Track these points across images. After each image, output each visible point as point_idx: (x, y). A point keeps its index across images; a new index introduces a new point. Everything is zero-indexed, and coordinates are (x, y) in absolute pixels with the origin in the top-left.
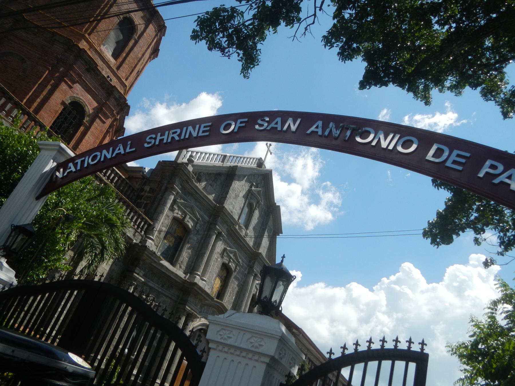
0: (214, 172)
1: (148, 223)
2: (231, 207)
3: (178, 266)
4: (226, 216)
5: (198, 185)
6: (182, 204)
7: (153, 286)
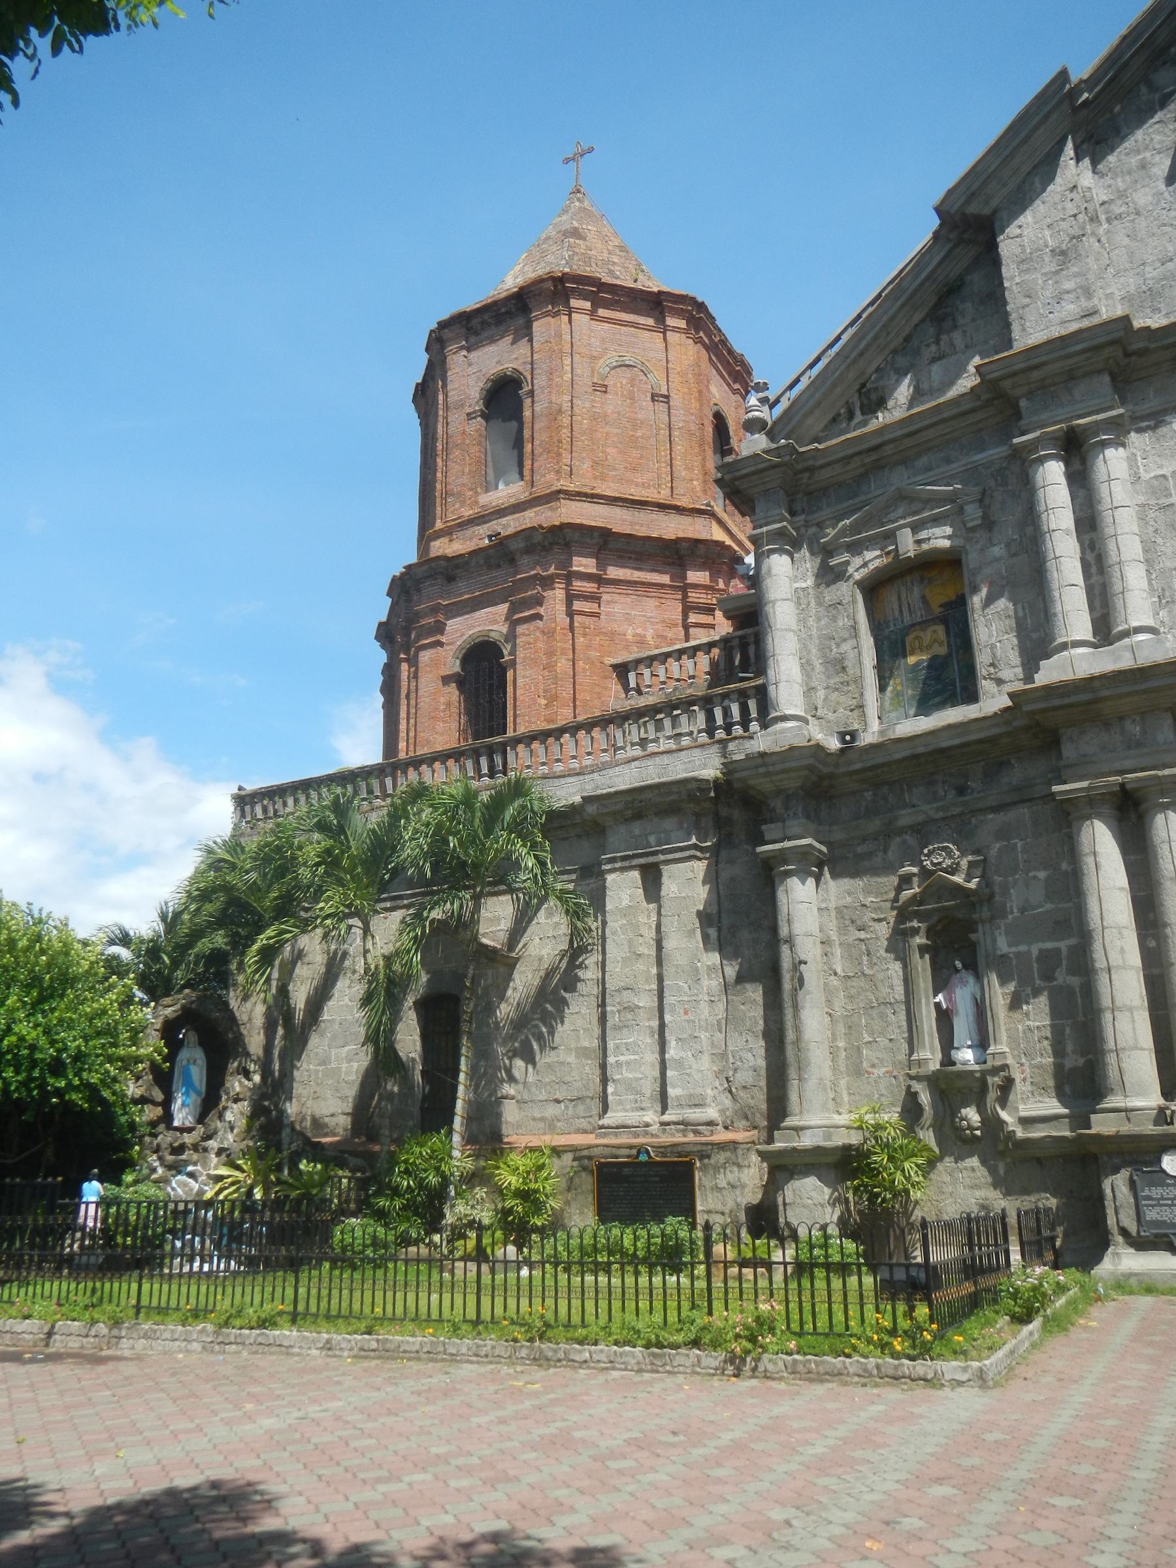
0: (918, 317)
1: (753, 692)
2: (1070, 308)
3: (986, 685)
4: (1036, 367)
5: (882, 418)
6: (855, 529)
7: (920, 818)
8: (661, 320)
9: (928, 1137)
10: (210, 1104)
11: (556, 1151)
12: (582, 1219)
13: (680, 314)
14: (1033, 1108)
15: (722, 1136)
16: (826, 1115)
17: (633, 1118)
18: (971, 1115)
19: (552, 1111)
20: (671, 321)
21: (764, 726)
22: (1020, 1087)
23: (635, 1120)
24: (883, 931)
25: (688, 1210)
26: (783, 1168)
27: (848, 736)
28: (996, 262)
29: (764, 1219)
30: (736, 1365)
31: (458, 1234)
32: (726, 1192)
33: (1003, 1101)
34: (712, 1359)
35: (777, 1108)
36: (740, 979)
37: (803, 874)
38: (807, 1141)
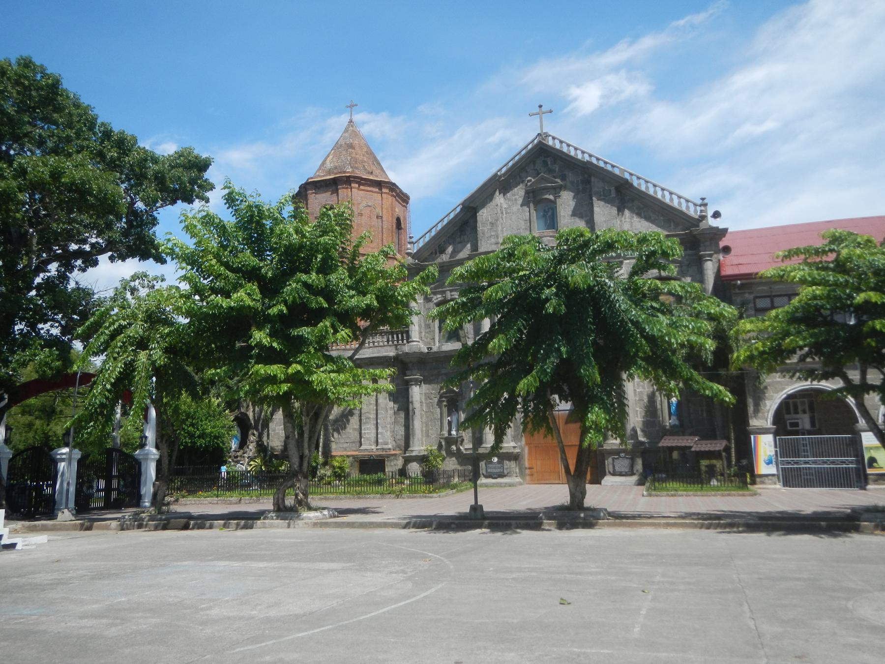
8: (381, 189)
9: (444, 453)
10: (243, 444)
11: (348, 456)
12: (355, 474)
13: (387, 187)
14: (467, 446)
15: (393, 452)
16: (419, 447)
17: (368, 447)
18: (454, 447)
19: (345, 445)
20: (384, 190)
21: (408, 342)
22: (465, 441)
23: (369, 448)
24: (436, 400)
25: (384, 471)
26: (408, 460)
27: (430, 349)
28: (476, 221)
29: (403, 473)
30: (398, 496)
31: (321, 478)
32: (393, 466)
33: (461, 444)
34: (393, 496)
35: (407, 445)
36: (398, 410)
37: (416, 385)
38: (414, 454)
